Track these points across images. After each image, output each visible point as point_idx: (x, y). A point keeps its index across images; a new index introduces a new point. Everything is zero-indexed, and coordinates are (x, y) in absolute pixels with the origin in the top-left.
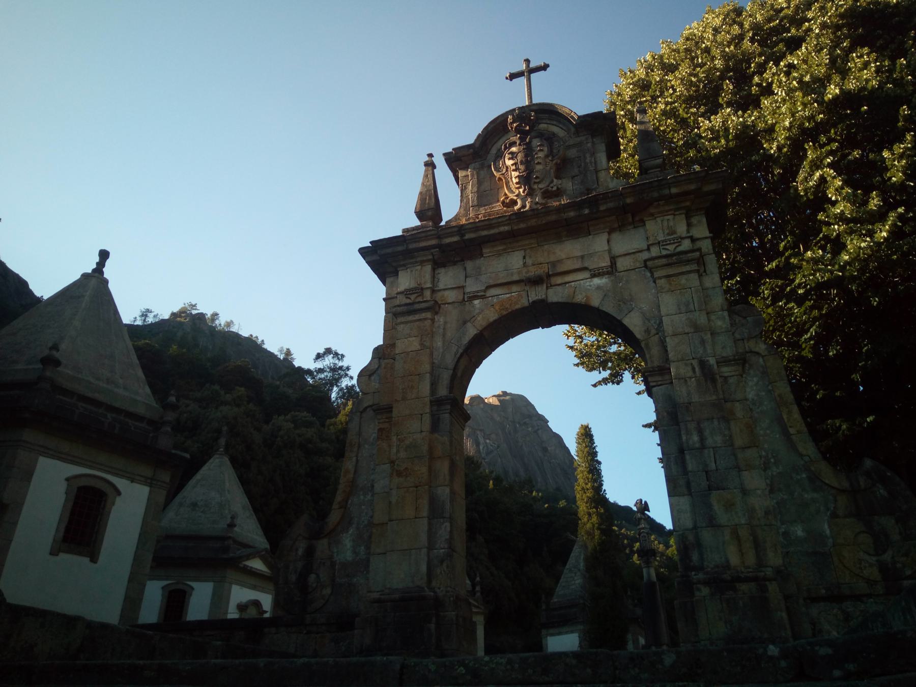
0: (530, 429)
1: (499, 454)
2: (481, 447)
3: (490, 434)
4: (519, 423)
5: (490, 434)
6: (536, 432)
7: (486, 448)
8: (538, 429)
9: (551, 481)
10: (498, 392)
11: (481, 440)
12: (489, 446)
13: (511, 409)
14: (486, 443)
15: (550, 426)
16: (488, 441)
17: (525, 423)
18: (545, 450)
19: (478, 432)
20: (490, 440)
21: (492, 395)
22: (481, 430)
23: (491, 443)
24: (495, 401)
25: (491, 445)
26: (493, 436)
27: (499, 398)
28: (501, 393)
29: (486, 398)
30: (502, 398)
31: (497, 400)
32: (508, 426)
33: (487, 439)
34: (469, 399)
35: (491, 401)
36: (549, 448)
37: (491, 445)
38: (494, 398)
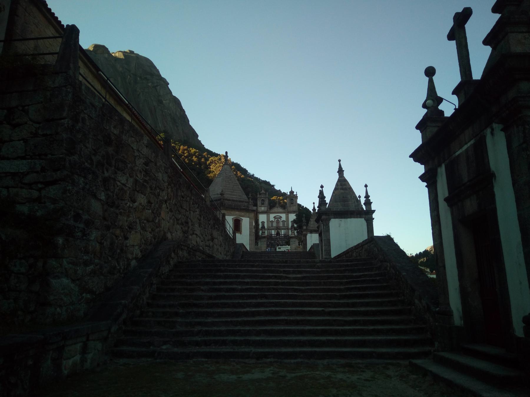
0: (150, 84)
8: (157, 86)
9: (160, 125)
10: (127, 50)
13: (134, 64)
15: (169, 88)
18: (160, 102)
21: (119, 51)
24: (121, 56)
27: (125, 54)
28: (128, 51)
29: (114, 53)
30: (125, 54)
31: (122, 54)
32: (129, 77)
34: (94, 46)
35: (117, 55)
36: (164, 102)
38: (120, 53)
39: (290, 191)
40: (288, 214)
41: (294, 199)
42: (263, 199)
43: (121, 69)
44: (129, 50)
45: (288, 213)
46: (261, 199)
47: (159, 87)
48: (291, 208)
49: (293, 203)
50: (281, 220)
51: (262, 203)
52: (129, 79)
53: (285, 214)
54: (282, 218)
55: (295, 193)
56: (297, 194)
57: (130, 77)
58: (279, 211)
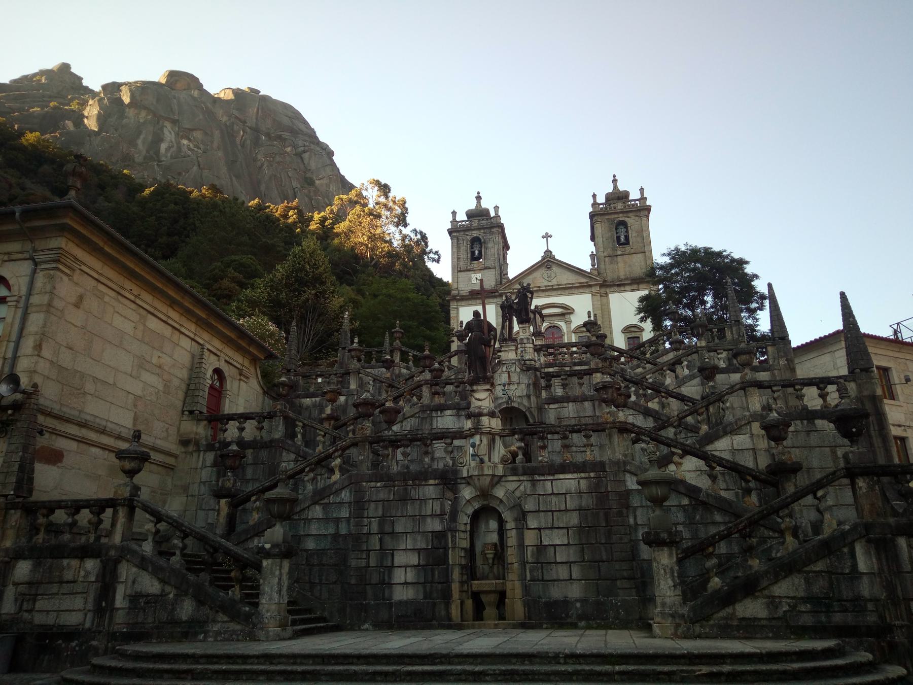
0: (289, 149)
1: (198, 161)
2: (163, 146)
3: (192, 130)
4: (268, 135)
5: (192, 130)
6: (299, 155)
7: (174, 149)
8: (304, 152)
10: (244, 87)
11: (169, 134)
12: (184, 149)
13: (256, 110)
14: (179, 143)
16: (185, 142)
17: (280, 137)
19: (168, 124)
20: (189, 140)
22: (174, 122)
23: (192, 146)
24: (230, 96)
25: (190, 149)
26: (198, 135)
32: (242, 132)
33: (182, 138)
36: (317, 182)
37: (190, 149)
39: (610, 189)
40: (607, 295)
41: (630, 221)
42: (475, 234)
43: (225, 119)
44: (249, 88)
45: (603, 290)
46: (469, 238)
47: (308, 153)
48: (621, 265)
49: (627, 238)
50: (569, 322)
51: (473, 253)
52: (242, 137)
53: (589, 296)
54: (572, 317)
55: (634, 195)
56: (643, 199)
57: (244, 132)
58: (554, 282)
